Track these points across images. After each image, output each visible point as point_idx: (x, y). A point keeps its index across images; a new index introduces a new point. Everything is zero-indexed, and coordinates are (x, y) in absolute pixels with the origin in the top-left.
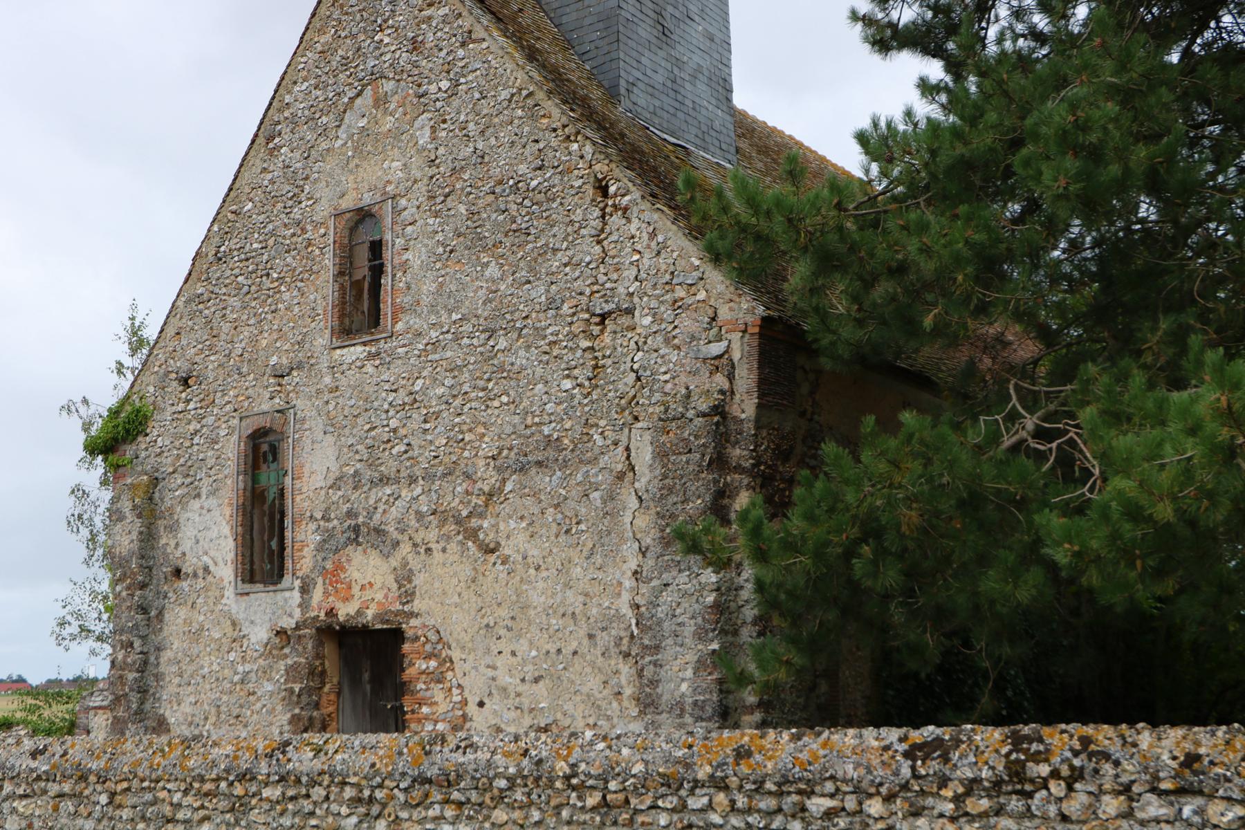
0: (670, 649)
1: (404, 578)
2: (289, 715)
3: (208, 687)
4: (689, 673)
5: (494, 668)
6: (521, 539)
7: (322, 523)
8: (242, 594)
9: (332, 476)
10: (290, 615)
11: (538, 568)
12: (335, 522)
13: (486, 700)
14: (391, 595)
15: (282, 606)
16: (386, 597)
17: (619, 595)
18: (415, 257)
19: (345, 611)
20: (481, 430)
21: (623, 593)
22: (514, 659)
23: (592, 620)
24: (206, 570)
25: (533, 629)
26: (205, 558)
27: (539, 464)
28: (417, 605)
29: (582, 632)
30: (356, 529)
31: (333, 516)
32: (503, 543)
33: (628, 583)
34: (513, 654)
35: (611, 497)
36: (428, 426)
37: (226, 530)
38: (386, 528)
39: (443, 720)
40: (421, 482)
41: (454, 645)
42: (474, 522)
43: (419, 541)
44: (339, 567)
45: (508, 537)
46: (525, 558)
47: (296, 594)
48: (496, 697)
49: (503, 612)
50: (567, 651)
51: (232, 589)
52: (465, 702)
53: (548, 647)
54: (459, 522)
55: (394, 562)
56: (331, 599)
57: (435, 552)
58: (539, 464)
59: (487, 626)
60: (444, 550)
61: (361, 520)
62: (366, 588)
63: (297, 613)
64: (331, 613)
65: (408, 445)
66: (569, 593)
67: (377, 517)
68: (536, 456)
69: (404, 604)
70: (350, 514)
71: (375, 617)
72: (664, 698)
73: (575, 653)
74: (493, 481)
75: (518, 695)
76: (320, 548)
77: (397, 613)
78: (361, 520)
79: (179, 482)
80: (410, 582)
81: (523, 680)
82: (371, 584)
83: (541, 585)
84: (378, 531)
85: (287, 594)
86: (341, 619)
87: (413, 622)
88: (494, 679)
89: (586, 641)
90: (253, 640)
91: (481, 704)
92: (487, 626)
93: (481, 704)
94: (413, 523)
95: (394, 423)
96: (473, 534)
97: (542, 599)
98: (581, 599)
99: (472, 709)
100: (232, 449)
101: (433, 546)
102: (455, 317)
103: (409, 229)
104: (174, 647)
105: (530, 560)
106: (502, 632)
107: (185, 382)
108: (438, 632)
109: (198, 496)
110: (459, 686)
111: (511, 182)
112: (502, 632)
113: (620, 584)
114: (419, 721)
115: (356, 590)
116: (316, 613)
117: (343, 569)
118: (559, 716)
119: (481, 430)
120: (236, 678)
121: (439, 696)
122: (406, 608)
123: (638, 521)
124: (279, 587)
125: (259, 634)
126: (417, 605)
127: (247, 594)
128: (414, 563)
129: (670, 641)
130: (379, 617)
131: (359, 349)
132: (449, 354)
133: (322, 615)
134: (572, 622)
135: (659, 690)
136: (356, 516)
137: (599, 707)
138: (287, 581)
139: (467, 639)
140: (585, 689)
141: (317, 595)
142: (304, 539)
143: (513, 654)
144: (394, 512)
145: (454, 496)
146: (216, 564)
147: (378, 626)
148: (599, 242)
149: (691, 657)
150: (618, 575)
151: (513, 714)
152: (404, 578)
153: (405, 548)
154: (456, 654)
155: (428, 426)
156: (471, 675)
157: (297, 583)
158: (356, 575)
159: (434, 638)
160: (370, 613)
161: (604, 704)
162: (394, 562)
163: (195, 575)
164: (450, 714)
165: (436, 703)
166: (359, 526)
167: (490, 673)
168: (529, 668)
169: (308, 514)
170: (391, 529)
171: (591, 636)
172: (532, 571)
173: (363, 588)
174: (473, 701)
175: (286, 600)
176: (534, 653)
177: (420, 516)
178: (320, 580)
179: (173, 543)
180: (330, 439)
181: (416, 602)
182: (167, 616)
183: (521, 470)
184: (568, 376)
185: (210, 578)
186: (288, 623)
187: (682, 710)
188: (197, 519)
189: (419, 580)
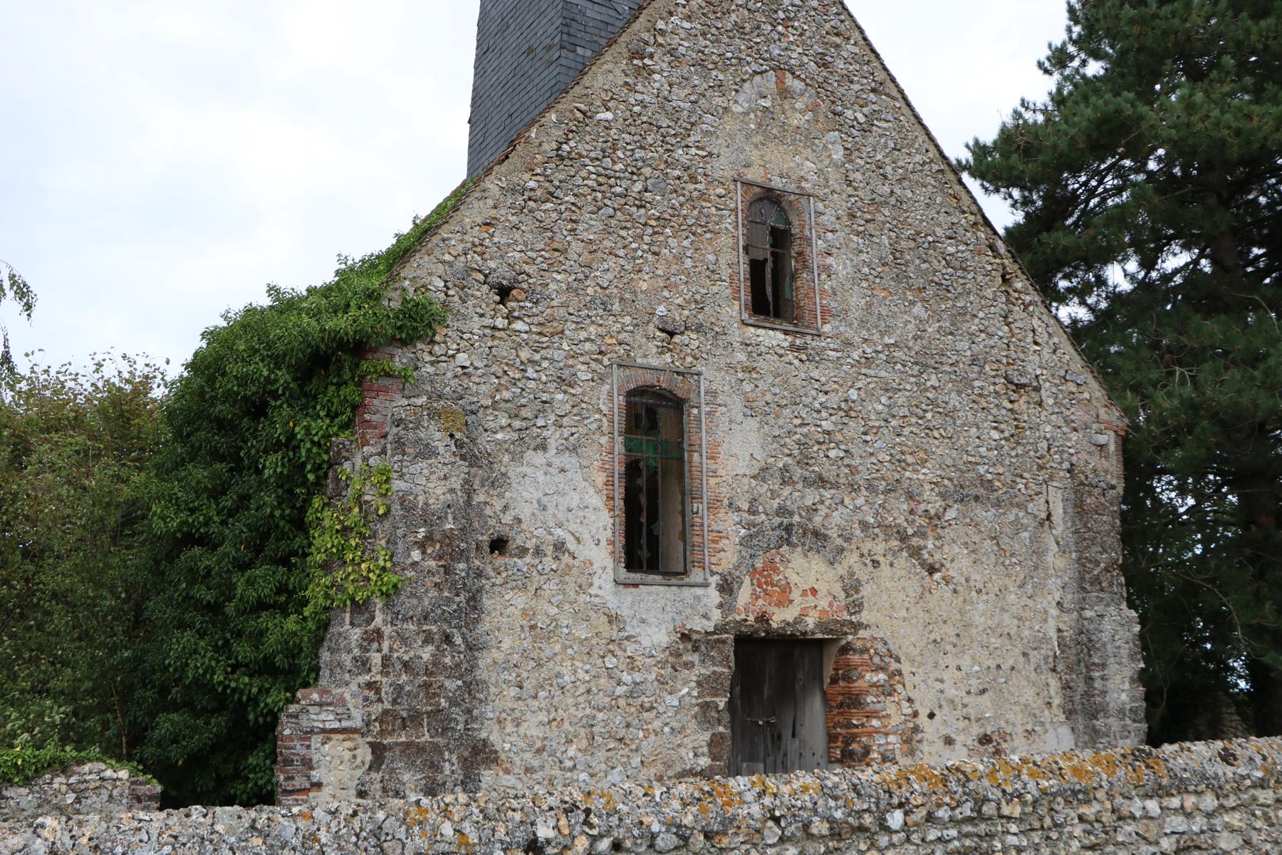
0: (1113, 667)
1: (852, 586)
2: (707, 736)
3: (570, 701)
4: (1127, 686)
5: (942, 681)
6: (964, 562)
7: (746, 515)
8: (626, 585)
9: (757, 466)
10: (705, 616)
11: (979, 592)
12: (763, 517)
13: (936, 712)
14: (835, 604)
15: (701, 606)
16: (831, 605)
17: (1046, 620)
18: (841, 266)
19: (780, 617)
20: (922, 455)
21: (1050, 619)
22: (959, 673)
23: (1025, 641)
24: (559, 547)
25: (975, 645)
26: (559, 531)
27: (977, 498)
28: (865, 617)
29: (1017, 651)
30: (788, 529)
31: (761, 509)
32: (948, 565)
33: (1054, 612)
34: (959, 668)
35: (1035, 539)
36: (868, 438)
37: (597, 501)
38: (829, 532)
39: (895, 733)
40: (865, 493)
41: (903, 659)
42: (915, 541)
43: (865, 552)
44: (771, 566)
45: (952, 561)
46: (967, 581)
47: (713, 596)
48: (946, 709)
49: (950, 631)
50: (1006, 666)
51: (610, 575)
52: (915, 714)
53: (989, 663)
54: (903, 538)
55: (841, 570)
56: (761, 602)
57: (883, 565)
58: (977, 498)
59: (935, 641)
60: (891, 565)
61: (796, 518)
62: (806, 593)
63: (716, 615)
64: (763, 618)
65: (846, 451)
66: (1006, 616)
67: (818, 519)
68: (970, 491)
69: (852, 614)
70: (782, 511)
71: (817, 625)
72: (1111, 705)
73: (1013, 668)
74: (937, 505)
75: (965, 706)
76: (745, 542)
77: (843, 623)
78: (796, 518)
79: (504, 422)
80: (857, 592)
81: (969, 693)
82: (814, 591)
83: (981, 607)
84: (816, 534)
85: (699, 591)
86: (774, 625)
87: (862, 633)
88: (942, 692)
89: (1021, 659)
90: (646, 642)
91: (931, 716)
92: (935, 641)
93: (931, 716)
94: (858, 532)
95: (826, 425)
96: (915, 553)
97: (983, 619)
98: (1015, 622)
99: (923, 720)
100: (608, 402)
101: (881, 559)
102: (887, 340)
103: (829, 234)
104: (505, 646)
105: (972, 583)
106: (949, 648)
107: (504, 293)
108: (886, 643)
109: (543, 447)
110: (910, 700)
111: (930, 239)
112: (949, 648)
113: (1046, 612)
114: (869, 734)
115: (796, 595)
116: (743, 616)
117: (776, 570)
118: (1003, 724)
119: (922, 455)
120: (620, 690)
121: (892, 709)
122: (853, 618)
123: (1058, 563)
124: (687, 580)
125: (657, 636)
126: (865, 617)
127: (636, 585)
128: (862, 574)
129: (1112, 660)
130: (821, 625)
131: (782, 336)
132: (883, 374)
133: (751, 618)
134: (1007, 642)
135: (1107, 699)
136: (791, 514)
137: (1035, 715)
138: (696, 575)
139: (916, 653)
140: (1022, 700)
141: (744, 595)
142: (722, 534)
143: (959, 668)
144: (836, 517)
145: (898, 511)
146: (578, 540)
147: (819, 636)
148: (1008, 324)
149: (1128, 672)
150: (1045, 604)
151: (962, 724)
152: (852, 586)
153: (852, 559)
154: (906, 668)
155: (868, 438)
156: (921, 687)
157: (714, 580)
158: (794, 578)
159: (883, 650)
160: (811, 622)
161: (1037, 712)
162: (841, 570)
163: (538, 552)
164: (902, 727)
165: (888, 716)
166: (791, 525)
167: (939, 686)
168: (974, 682)
169: (726, 502)
170: (833, 533)
171: (1025, 654)
172: (974, 593)
173: (804, 593)
174: (924, 713)
175: (698, 598)
176: (977, 668)
177: (864, 526)
178: (747, 580)
179: (498, 505)
180: (753, 424)
181: (864, 613)
182: (487, 602)
183: (962, 500)
184: (995, 428)
185: (566, 558)
186: (698, 625)
187: (1124, 714)
188: (541, 478)
189: (866, 591)
